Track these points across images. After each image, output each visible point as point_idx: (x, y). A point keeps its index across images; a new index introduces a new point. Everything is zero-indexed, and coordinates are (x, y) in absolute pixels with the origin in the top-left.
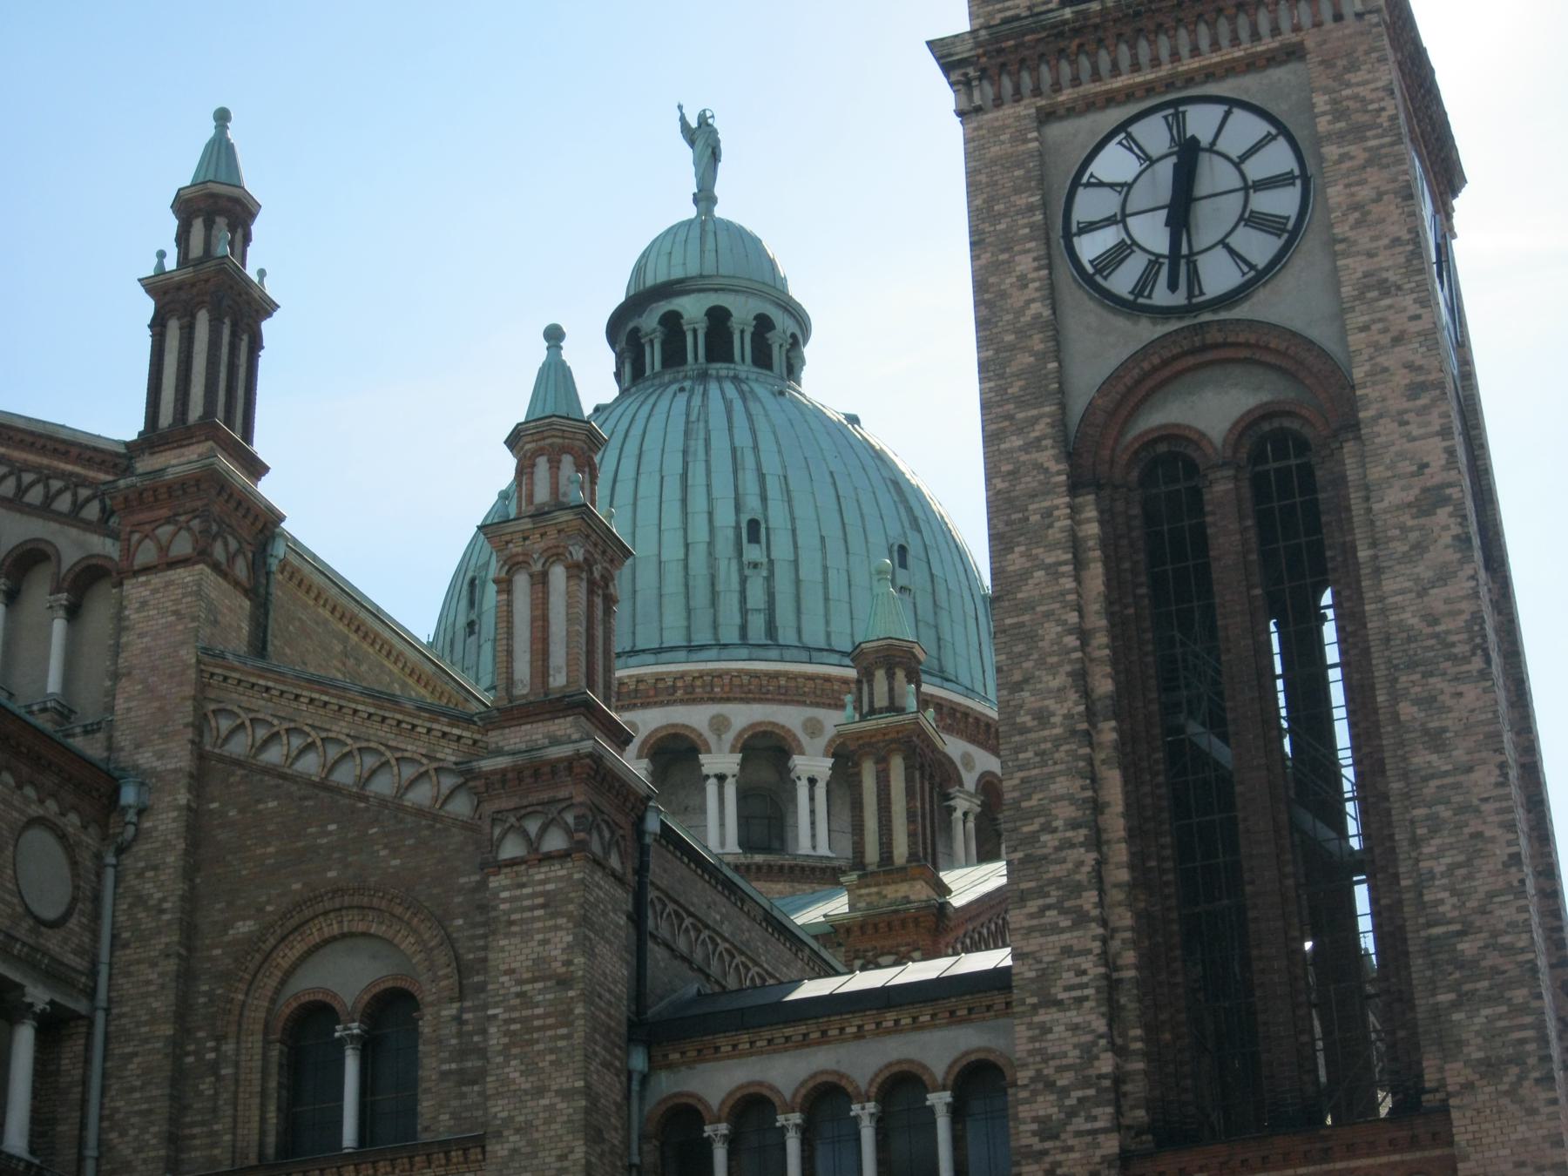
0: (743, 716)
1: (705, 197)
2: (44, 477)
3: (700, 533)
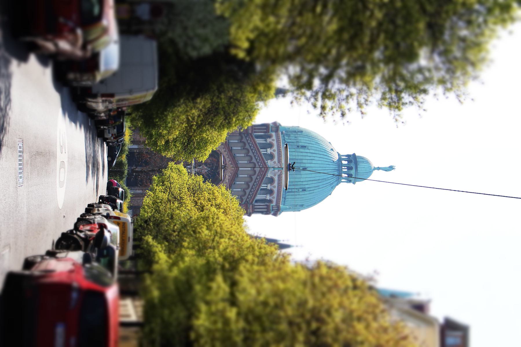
0: (275, 190)
1: (379, 169)
2: (253, 194)
3: (304, 183)
